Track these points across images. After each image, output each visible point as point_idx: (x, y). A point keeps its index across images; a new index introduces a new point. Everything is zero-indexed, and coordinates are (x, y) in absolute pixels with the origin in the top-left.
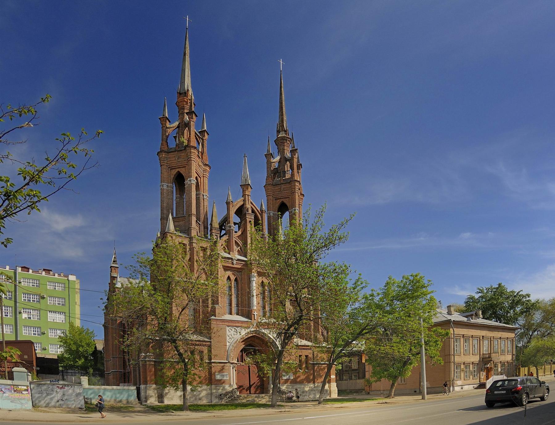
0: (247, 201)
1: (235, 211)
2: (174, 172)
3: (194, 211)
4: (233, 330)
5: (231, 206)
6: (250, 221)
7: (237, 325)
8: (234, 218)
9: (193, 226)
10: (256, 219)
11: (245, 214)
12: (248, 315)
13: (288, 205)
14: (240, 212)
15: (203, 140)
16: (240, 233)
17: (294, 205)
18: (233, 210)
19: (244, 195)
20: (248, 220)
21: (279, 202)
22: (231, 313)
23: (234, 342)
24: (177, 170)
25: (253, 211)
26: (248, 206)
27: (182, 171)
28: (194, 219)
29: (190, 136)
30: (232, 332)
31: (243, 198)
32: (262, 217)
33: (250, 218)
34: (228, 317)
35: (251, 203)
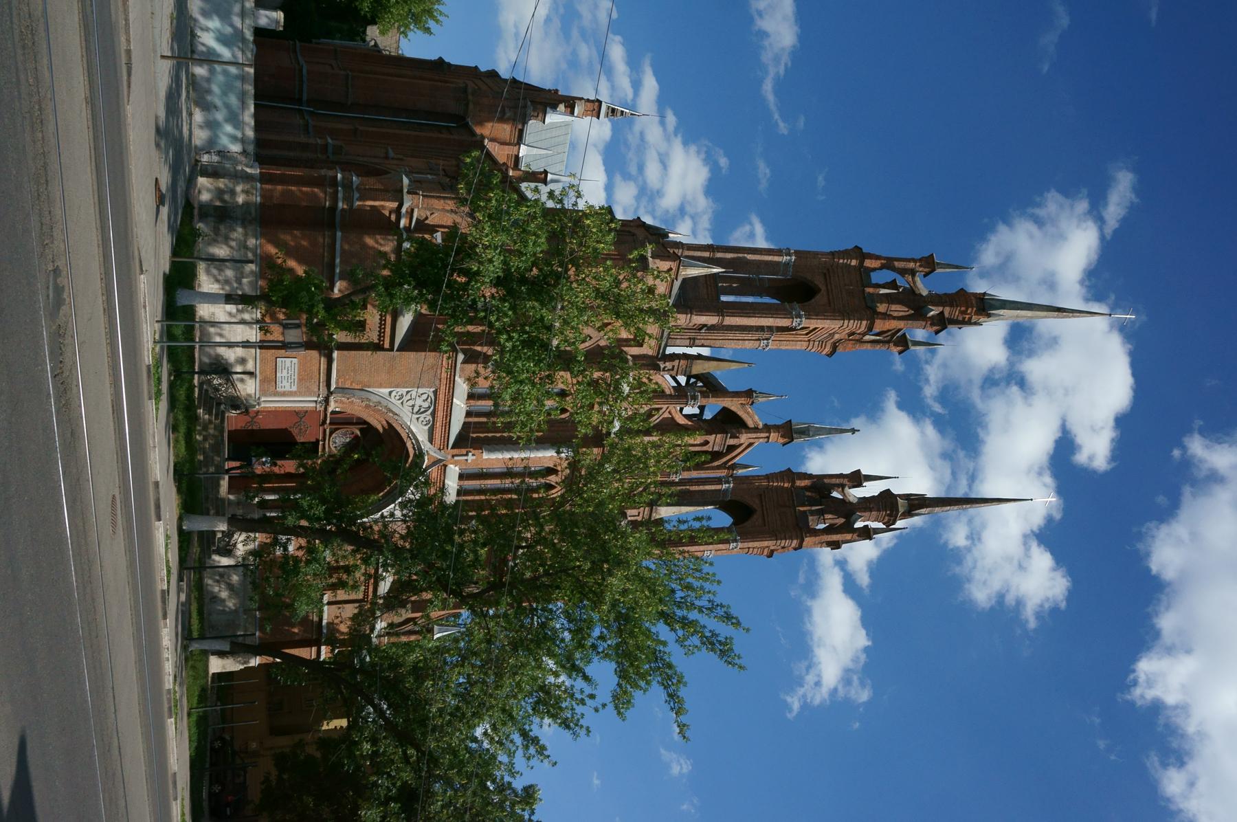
0: (754, 435)
1: (733, 408)
2: (819, 281)
3: (729, 321)
4: (426, 405)
5: (742, 400)
6: (707, 443)
7: (440, 414)
8: (713, 406)
9: (694, 317)
10: (716, 455)
11: (724, 432)
12: (465, 441)
13: (748, 524)
14: (729, 422)
15: (888, 342)
16: (682, 421)
17: (746, 536)
18: (733, 405)
19: (767, 428)
20: (711, 438)
21: (754, 503)
22: (471, 396)
23: (390, 406)
24: (823, 288)
25: (731, 448)
26: (744, 438)
27: (821, 299)
28: (712, 320)
29: (894, 318)
30: (419, 402)
31: (761, 426)
32: (718, 467)
33: (716, 441)
34: (462, 388)
35: (750, 445)
